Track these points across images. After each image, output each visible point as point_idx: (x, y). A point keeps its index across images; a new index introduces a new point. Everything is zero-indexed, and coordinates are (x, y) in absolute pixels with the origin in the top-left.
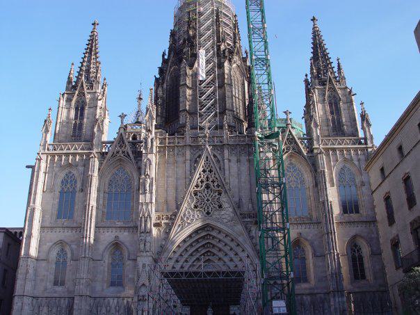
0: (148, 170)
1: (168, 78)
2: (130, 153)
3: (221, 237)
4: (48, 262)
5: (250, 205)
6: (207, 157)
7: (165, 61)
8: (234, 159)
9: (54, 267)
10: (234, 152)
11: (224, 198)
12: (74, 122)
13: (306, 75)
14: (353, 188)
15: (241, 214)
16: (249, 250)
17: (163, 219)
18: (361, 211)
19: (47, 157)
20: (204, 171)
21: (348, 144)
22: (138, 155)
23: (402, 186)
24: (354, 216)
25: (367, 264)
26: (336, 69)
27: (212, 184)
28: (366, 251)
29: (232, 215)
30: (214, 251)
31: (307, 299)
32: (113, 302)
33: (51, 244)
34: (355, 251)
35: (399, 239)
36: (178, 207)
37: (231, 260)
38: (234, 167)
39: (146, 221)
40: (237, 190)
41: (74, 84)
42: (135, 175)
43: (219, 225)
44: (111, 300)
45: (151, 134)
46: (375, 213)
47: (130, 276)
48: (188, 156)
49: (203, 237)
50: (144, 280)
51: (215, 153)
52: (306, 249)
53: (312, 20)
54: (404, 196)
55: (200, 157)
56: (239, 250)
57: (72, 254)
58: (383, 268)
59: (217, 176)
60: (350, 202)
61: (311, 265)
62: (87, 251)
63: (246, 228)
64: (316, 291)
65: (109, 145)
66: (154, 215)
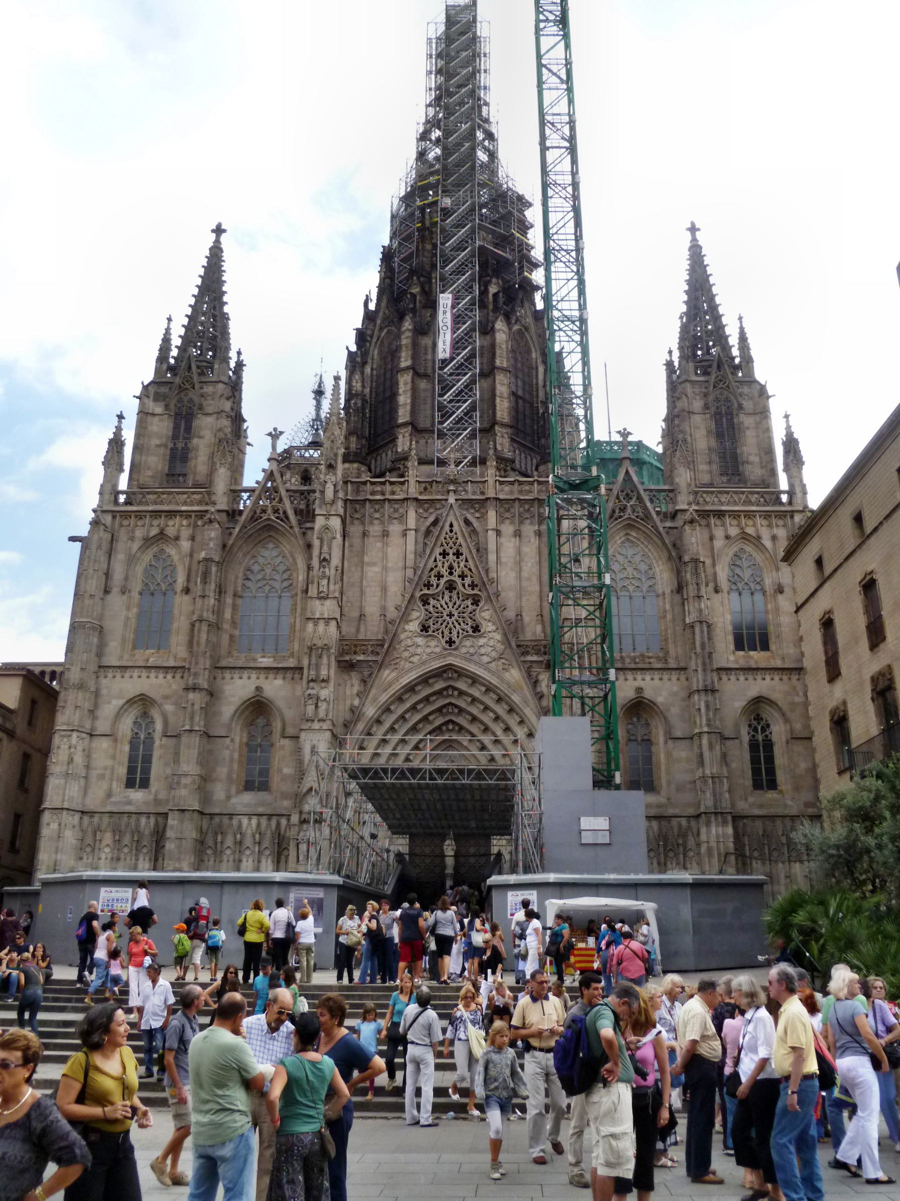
0: (325, 548)
1: (375, 353)
2: (291, 513)
3: (476, 692)
4: (116, 740)
6: (451, 525)
7: (369, 317)
9: (127, 748)
10: (507, 515)
11: (485, 615)
12: (170, 445)
13: (670, 352)
14: (758, 597)
15: (518, 646)
17: (355, 653)
18: (773, 647)
19: (114, 517)
20: (444, 554)
21: (750, 503)
24: (757, 657)
25: (780, 758)
27: (459, 581)
28: (778, 732)
29: (500, 647)
30: (461, 720)
32: (249, 825)
33: (121, 702)
34: (755, 730)
35: (845, 711)
38: (509, 545)
39: (320, 657)
41: (172, 361)
42: (301, 564)
43: (472, 668)
44: (245, 821)
45: (335, 474)
46: (802, 654)
48: (412, 522)
49: (439, 693)
51: (469, 517)
52: (653, 723)
53: (688, 229)
54: (862, 621)
56: (512, 721)
57: (166, 723)
58: (814, 768)
59: (471, 564)
60: (751, 627)
61: (662, 756)
62: (197, 718)
63: (529, 676)
64: (671, 811)
65: (245, 496)
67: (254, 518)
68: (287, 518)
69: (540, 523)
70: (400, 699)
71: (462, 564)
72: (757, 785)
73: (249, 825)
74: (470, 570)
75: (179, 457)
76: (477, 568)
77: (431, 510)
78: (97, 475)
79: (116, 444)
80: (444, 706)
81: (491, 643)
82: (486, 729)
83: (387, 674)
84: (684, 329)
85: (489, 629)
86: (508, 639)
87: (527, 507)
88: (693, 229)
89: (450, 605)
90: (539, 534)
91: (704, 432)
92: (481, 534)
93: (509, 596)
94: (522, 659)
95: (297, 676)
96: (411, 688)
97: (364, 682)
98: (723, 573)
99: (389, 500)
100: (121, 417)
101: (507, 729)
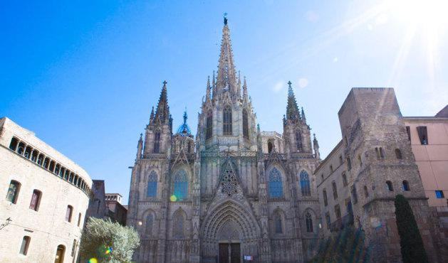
8: (244, 164)
16: (251, 214)
23: (331, 187)
26: (301, 113)
28: (313, 217)
31: (282, 242)
42: (190, 173)
48: (218, 163)
50: (196, 231)
67: (178, 162)
70: (216, 210)
72: (308, 231)
73: (179, 243)
75: (156, 147)
78: (136, 151)
79: (141, 141)
82: (239, 217)
83: (213, 204)
84: (288, 111)
88: (290, 83)
90: (251, 166)
91: (293, 138)
93: (244, 182)
96: (219, 207)
97: (208, 205)
98: (298, 175)
100: (141, 135)
101: (244, 217)
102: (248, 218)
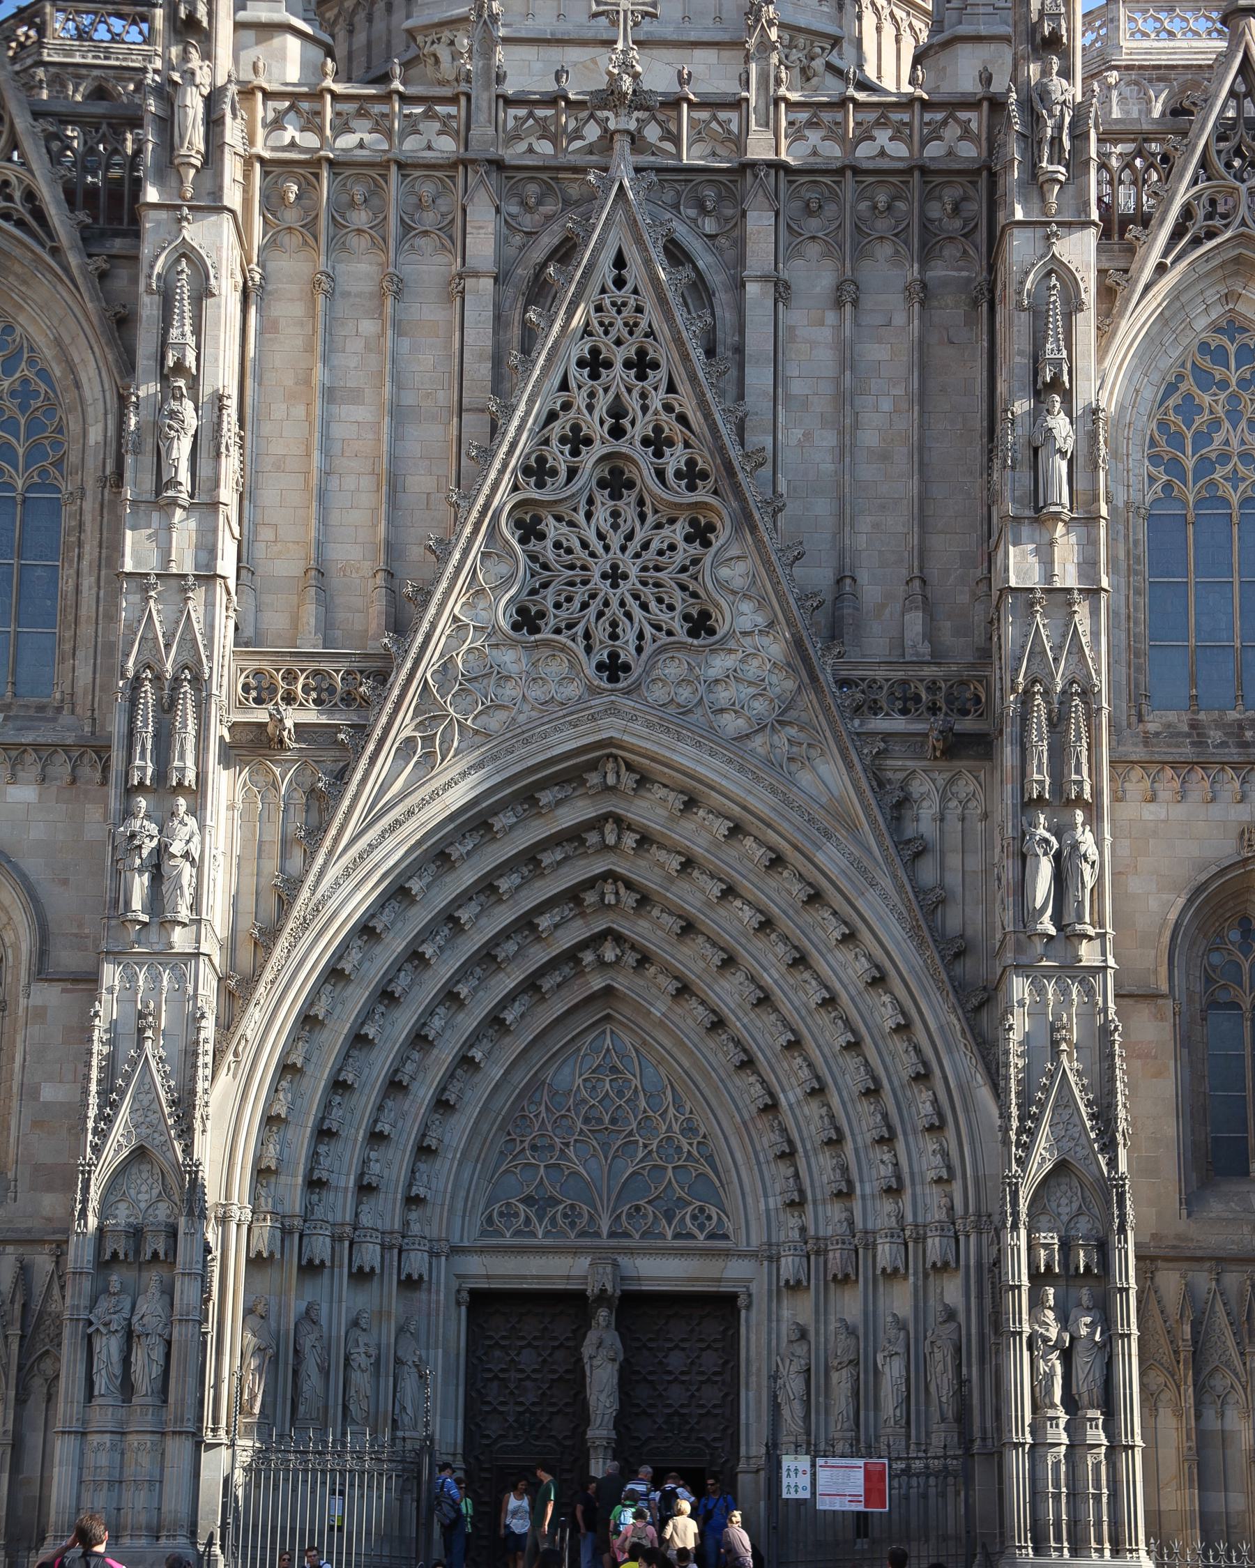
3: (700, 834)
5: (915, 622)
6: (620, 262)
8: (815, 275)
10: (813, 224)
15: (843, 683)
16: (890, 932)
17: (289, 699)
20: (595, 363)
22: (111, 214)
27: (644, 459)
29: (784, 684)
30: (642, 930)
36: (400, 624)
37: (764, 1000)
40: (823, 508)
42: (94, 382)
43: (686, 755)
47: (49, 1093)
48: (482, 243)
49: (573, 837)
55: (565, 252)
59: (686, 402)
66: (225, 670)
68: (39, 215)
69: (926, 255)
71: (656, 401)
74: (682, 419)
76: (708, 416)
77: (547, 209)
80: (590, 884)
81: (753, 669)
85: (745, 623)
86: (806, 660)
87: (882, 199)
89: (615, 540)
92: (722, 298)
94: (857, 722)
95: (90, 773)
99: (401, 166)
102: (846, 970)
